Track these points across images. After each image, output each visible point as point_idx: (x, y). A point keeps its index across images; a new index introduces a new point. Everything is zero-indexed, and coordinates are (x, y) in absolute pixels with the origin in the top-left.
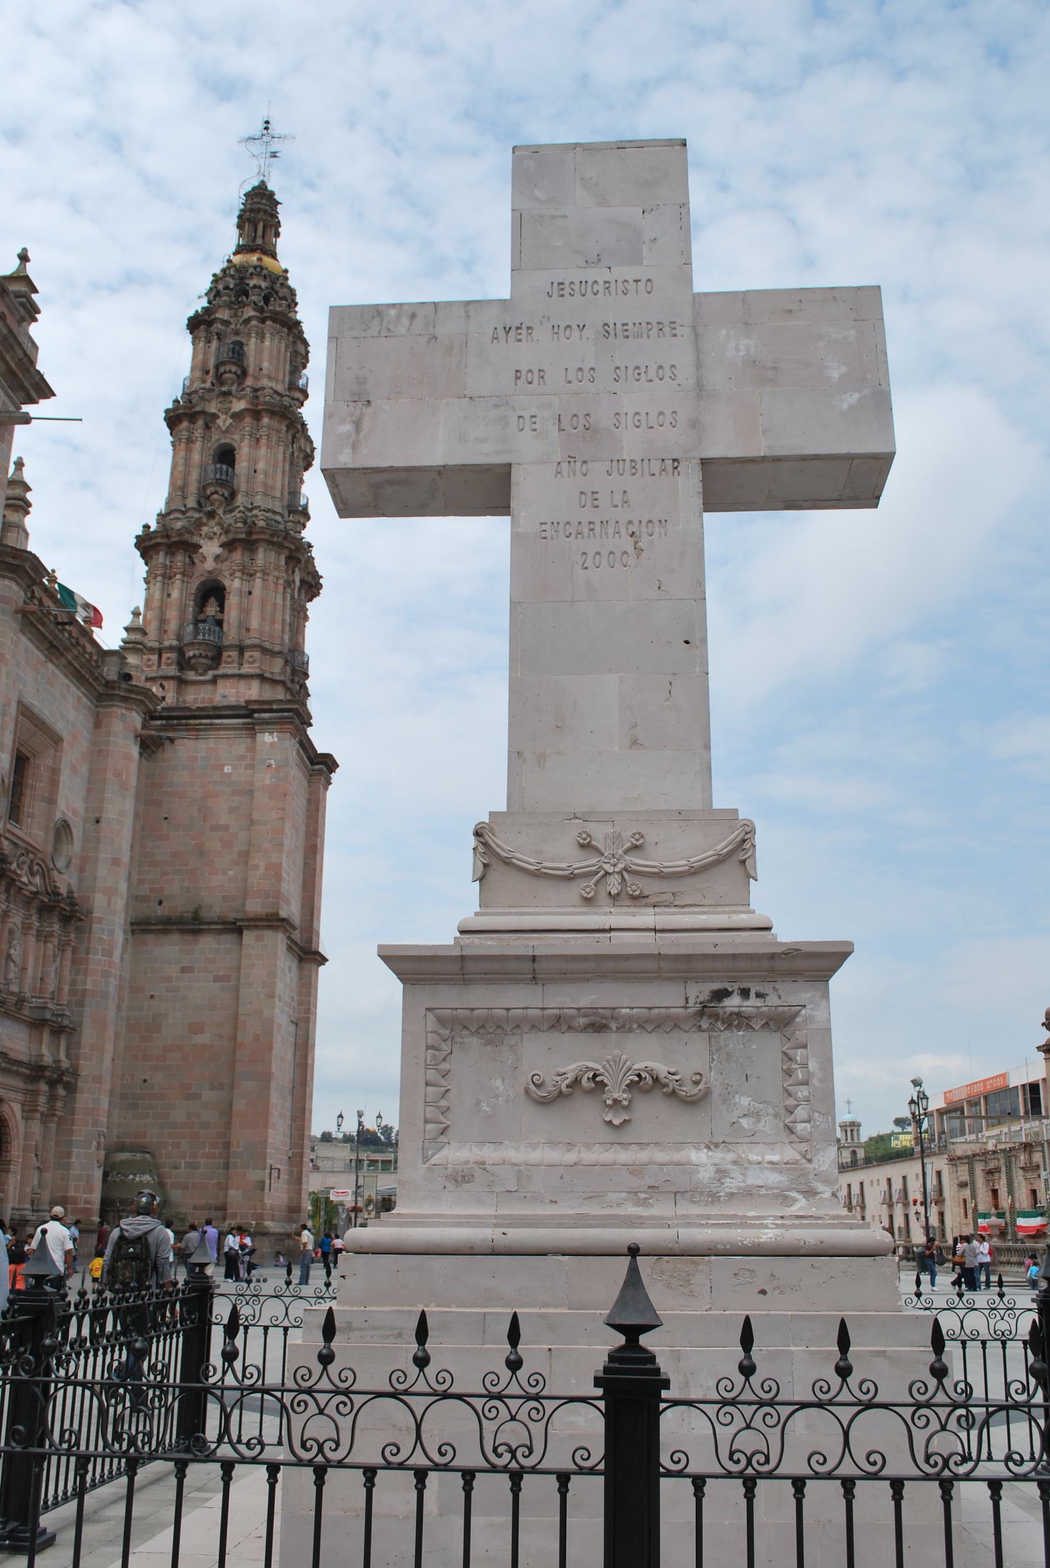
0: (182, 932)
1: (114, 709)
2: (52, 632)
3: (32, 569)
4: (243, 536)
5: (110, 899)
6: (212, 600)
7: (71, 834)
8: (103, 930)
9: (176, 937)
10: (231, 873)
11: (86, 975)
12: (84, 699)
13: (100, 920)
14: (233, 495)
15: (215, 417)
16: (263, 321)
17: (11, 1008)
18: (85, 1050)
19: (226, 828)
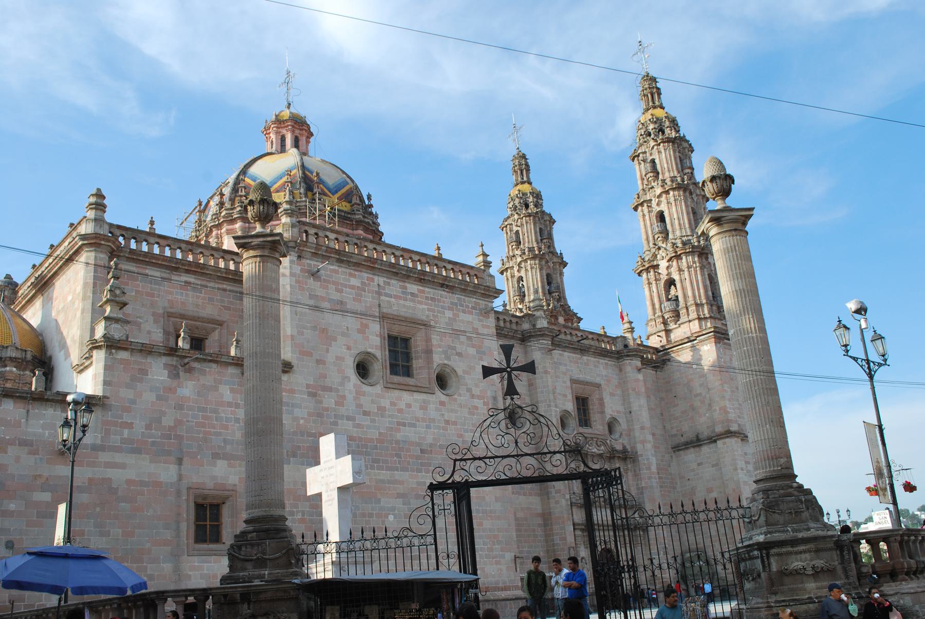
0: (694, 447)
1: (626, 361)
2: (578, 345)
4: (674, 255)
5: (644, 445)
6: (672, 286)
9: (692, 450)
10: (707, 415)
11: (641, 480)
12: (609, 363)
13: (641, 455)
14: (668, 234)
15: (651, 200)
16: (659, 145)
19: (700, 394)
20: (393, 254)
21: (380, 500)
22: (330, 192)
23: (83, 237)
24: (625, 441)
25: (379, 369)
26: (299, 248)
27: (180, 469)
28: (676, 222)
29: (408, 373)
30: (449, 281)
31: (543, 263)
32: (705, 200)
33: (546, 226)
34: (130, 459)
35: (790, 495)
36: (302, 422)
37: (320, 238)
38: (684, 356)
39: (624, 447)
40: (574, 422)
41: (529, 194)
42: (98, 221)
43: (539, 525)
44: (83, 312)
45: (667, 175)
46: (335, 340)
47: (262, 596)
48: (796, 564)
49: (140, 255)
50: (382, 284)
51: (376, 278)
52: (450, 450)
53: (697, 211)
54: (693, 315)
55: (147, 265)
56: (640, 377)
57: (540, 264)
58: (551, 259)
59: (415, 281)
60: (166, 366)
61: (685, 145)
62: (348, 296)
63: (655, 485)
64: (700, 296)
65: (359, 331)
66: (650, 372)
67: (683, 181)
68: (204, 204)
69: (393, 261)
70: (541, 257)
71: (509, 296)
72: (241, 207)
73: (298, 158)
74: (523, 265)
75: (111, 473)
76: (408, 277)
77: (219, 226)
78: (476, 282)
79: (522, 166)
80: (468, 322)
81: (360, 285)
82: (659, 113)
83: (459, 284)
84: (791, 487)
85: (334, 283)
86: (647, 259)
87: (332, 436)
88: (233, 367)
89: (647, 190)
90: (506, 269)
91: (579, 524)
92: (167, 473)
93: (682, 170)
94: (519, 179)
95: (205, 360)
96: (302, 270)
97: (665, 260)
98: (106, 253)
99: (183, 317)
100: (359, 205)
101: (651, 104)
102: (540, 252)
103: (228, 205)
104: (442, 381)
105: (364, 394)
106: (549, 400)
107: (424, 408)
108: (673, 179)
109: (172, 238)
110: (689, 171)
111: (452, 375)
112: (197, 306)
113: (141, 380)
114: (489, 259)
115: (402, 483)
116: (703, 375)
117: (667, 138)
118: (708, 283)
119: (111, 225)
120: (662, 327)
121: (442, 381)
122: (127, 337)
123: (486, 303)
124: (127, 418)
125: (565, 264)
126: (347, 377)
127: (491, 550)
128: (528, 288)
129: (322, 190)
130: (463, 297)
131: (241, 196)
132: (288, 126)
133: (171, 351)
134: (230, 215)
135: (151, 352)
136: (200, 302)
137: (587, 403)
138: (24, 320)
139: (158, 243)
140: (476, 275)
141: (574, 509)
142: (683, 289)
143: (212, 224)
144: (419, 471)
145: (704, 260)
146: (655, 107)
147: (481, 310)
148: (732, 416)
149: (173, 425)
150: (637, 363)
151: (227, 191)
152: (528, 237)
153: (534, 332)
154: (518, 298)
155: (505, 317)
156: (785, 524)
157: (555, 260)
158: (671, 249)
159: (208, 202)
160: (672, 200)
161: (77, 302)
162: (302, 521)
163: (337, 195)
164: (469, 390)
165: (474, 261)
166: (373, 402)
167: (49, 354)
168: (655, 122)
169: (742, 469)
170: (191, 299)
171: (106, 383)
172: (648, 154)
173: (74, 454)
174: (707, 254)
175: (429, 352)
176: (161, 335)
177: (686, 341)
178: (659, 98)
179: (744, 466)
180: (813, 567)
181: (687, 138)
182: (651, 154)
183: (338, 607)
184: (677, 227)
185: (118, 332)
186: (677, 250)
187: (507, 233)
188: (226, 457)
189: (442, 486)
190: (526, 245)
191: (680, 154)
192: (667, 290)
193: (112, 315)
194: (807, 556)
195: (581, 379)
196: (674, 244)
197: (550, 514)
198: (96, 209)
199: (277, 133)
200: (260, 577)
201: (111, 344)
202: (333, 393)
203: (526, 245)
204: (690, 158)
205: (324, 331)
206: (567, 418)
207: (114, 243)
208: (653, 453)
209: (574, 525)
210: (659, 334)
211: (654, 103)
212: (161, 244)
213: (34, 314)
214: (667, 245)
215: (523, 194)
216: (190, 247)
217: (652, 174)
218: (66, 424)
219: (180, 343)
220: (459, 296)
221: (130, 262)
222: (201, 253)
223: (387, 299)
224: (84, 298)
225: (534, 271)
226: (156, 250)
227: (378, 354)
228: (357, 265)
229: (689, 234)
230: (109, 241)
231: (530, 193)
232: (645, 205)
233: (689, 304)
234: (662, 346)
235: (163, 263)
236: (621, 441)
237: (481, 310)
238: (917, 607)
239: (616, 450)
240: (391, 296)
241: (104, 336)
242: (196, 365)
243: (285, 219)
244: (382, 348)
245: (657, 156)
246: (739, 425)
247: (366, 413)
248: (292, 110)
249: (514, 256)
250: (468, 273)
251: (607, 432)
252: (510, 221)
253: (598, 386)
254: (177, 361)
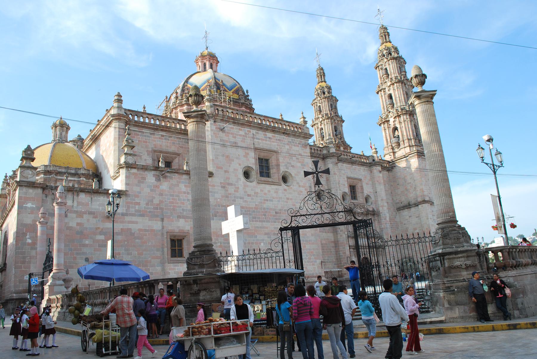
0: (407, 208)
4: (397, 115)
5: (383, 208)
6: (396, 131)
12: (366, 168)
13: (382, 213)
14: (394, 105)
15: (385, 88)
16: (389, 61)
19: (410, 183)
20: (260, 118)
21: (256, 236)
22: (228, 89)
23: (113, 116)
24: (374, 206)
25: (255, 174)
26: (214, 117)
27: (163, 224)
28: (398, 99)
29: (268, 175)
30: (287, 131)
31: (333, 121)
32: (412, 87)
33: (334, 103)
34: (139, 219)
35: (455, 230)
36: (219, 200)
37: (224, 112)
38: (402, 164)
39: (373, 209)
40: (349, 197)
41: (325, 87)
42: (119, 108)
43: (333, 247)
44: (114, 151)
45: (393, 76)
46: (233, 161)
47: (203, 281)
48: (457, 263)
49: (140, 123)
50: (254, 133)
51: (252, 130)
52: (289, 212)
53: (408, 93)
54: (406, 144)
55: (143, 128)
56: (381, 175)
57: (331, 122)
58: (337, 119)
59: (271, 131)
60: (154, 175)
61: (402, 60)
62: (239, 140)
63: (388, 227)
64: (410, 135)
65: (244, 156)
66: (385, 172)
67: (401, 79)
68: (168, 98)
69: (260, 122)
70: (331, 118)
71: (316, 137)
72: (186, 98)
73: (212, 74)
74: (323, 122)
75: (130, 226)
76: (267, 130)
77: (176, 108)
78: (300, 131)
79: (322, 74)
80: (297, 151)
81: (244, 134)
82: (389, 45)
83: (292, 132)
84: (455, 226)
85: (232, 134)
86: (383, 118)
87: (233, 206)
88: (185, 175)
89: (383, 83)
90: (315, 125)
91: (352, 246)
92: (157, 225)
93: (401, 73)
94: (320, 80)
95: (172, 172)
96: (216, 128)
97: (393, 118)
98: (123, 123)
99: (161, 152)
100: (242, 95)
101: (384, 40)
102: (331, 115)
103: (180, 98)
104: (285, 179)
105: (247, 186)
106: (337, 187)
107: (276, 192)
108: (396, 78)
109: (154, 115)
110: (404, 73)
111: (290, 177)
112: (167, 146)
113: (143, 183)
114: (306, 120)
115: (267, 228)
116: (411, 174)
117: (393, 57)
118: (414, 128)
119: (125, 110)
120: (391, 151)
121: (285, 179)
122: (135, 163)
123: (305, 141)
124: (137, 200)
125: (343, 121)
126: (239, 179)
127: (310, 259)
128: (326, 133)
129: (225, 89)
130: (294, 139)
131: (186, 93)
132: (207, 58)
133: (156, 168)
134: (181, 102)
135: (147, 169)
136: (169, 144)
137: (355, 188)
138: (87, 156)
139: (147, 117)
140: (300, 128)
141: (349, 239)
142: (402, 132)
143: (173, 107)
144: (275, 222)
145: (412, 117)
146: (386, 42)
147: (303, 145)
148: (426, 193)
149: (158, 203)
150: (379, 168)
151: (179, 91)
152: (325, 108)
153: (329, 155)
154: (321, 138)
155: (314, 148)
156: (452, 244)
157: (339, 119)
158: (396, 112)
159: (171, 97)
160: (396, 88)
161: (111, 147)
162: (220, 246)
163: (232, 91)
164: (298, 183)
165: (298, 120)
166: (252, 190)
167: (100, 171)
168: (387, 50)
169: (431, 219)
170: (164, 143)
171: (127, 184)
172: (383, 66)
173: (114, 217)
174: (413, 114)
175: (278, 165)
176: (151, 161)
177: (403, 157)
178: (389, 37)
179: (432, 218)
180: (466, 265)
181: (403, 57)
182: (385, 66)
183: (238, 286)
184: (398, 101)
185: (131, 160)
186: (399, 112)
187: (315, 107)
188: (184, 217)
189: (286, 229)
190: (324, 113)
191: (400, 65)
192: (394, 132)
193: (129, 152)
194: (463, 259)
195: (352, 177)
196: (397, 110)
197: (338, 241)
198: (118, 102)
199: (202, 62)
200: (202, 272)
201: (128, 166)
202: (233, 186)
203: (324, 113)
204: (404, 67)
205: (228, 157)
206: (345, 196)
207: (127, 118)
208: (388, 211)
209: (349, 246)
210: (390, 154)
211: (386, 40)
212: (149, 118)
213: (92, 153)
214: (393, 110)
215: (322, 88)
216: (163, 119)
217: (385, 76)
218: (109, 203)
219: (160, 165)
220: (292, 138)
221: (135, 127)
222: (168, 121)
223: (257, 140)
224: (115, 145)
225: (328, 125)
226: (147, 121)
227: (254, 167)
228: (243, 125)
229: (404, 104)
230: (125, 117)
231: (326, 87)
232: (382, 91)
233: (404, 139)
234: (391, 160)
235: (151, 127)
236: (372, 206)
237: (303, 145)
238: (516, 283)
239: (369, 211)
240: (259, 139)
241: (125, 162)
242: (168, 174)
243: (207, 104)
244: (256, 164)
245: (388, 66)
247: (249, 195)
248: (209, 50)
249: (318, 118)
250: (296, 127)
251: (365, 202)
252: (316, 101)
253: (360, 180)
254: (159, 173)
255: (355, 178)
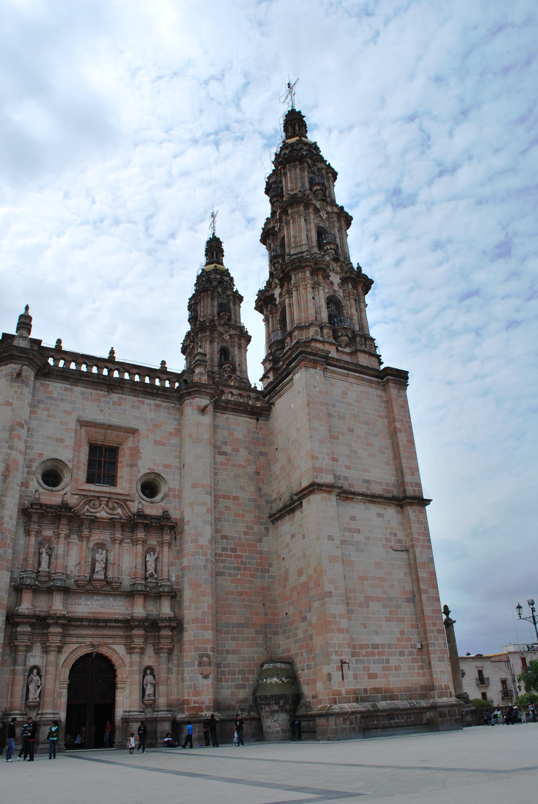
3: (21, 353)
7: (162, 477)
8: (190, 527)
17: (104, 589)
18: (186, 603)
39: (165, 512)
157: (232, 332)
169: (331, 538)
195: (98, 421)
236: (163, 504)
246: (336, 477)
253: (134, 431)
255: (109, 426)
